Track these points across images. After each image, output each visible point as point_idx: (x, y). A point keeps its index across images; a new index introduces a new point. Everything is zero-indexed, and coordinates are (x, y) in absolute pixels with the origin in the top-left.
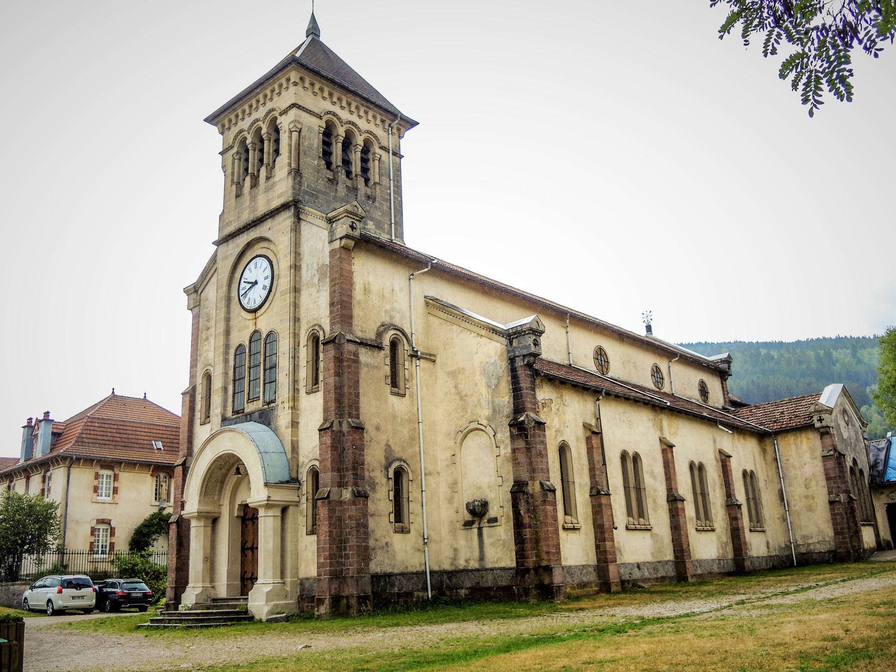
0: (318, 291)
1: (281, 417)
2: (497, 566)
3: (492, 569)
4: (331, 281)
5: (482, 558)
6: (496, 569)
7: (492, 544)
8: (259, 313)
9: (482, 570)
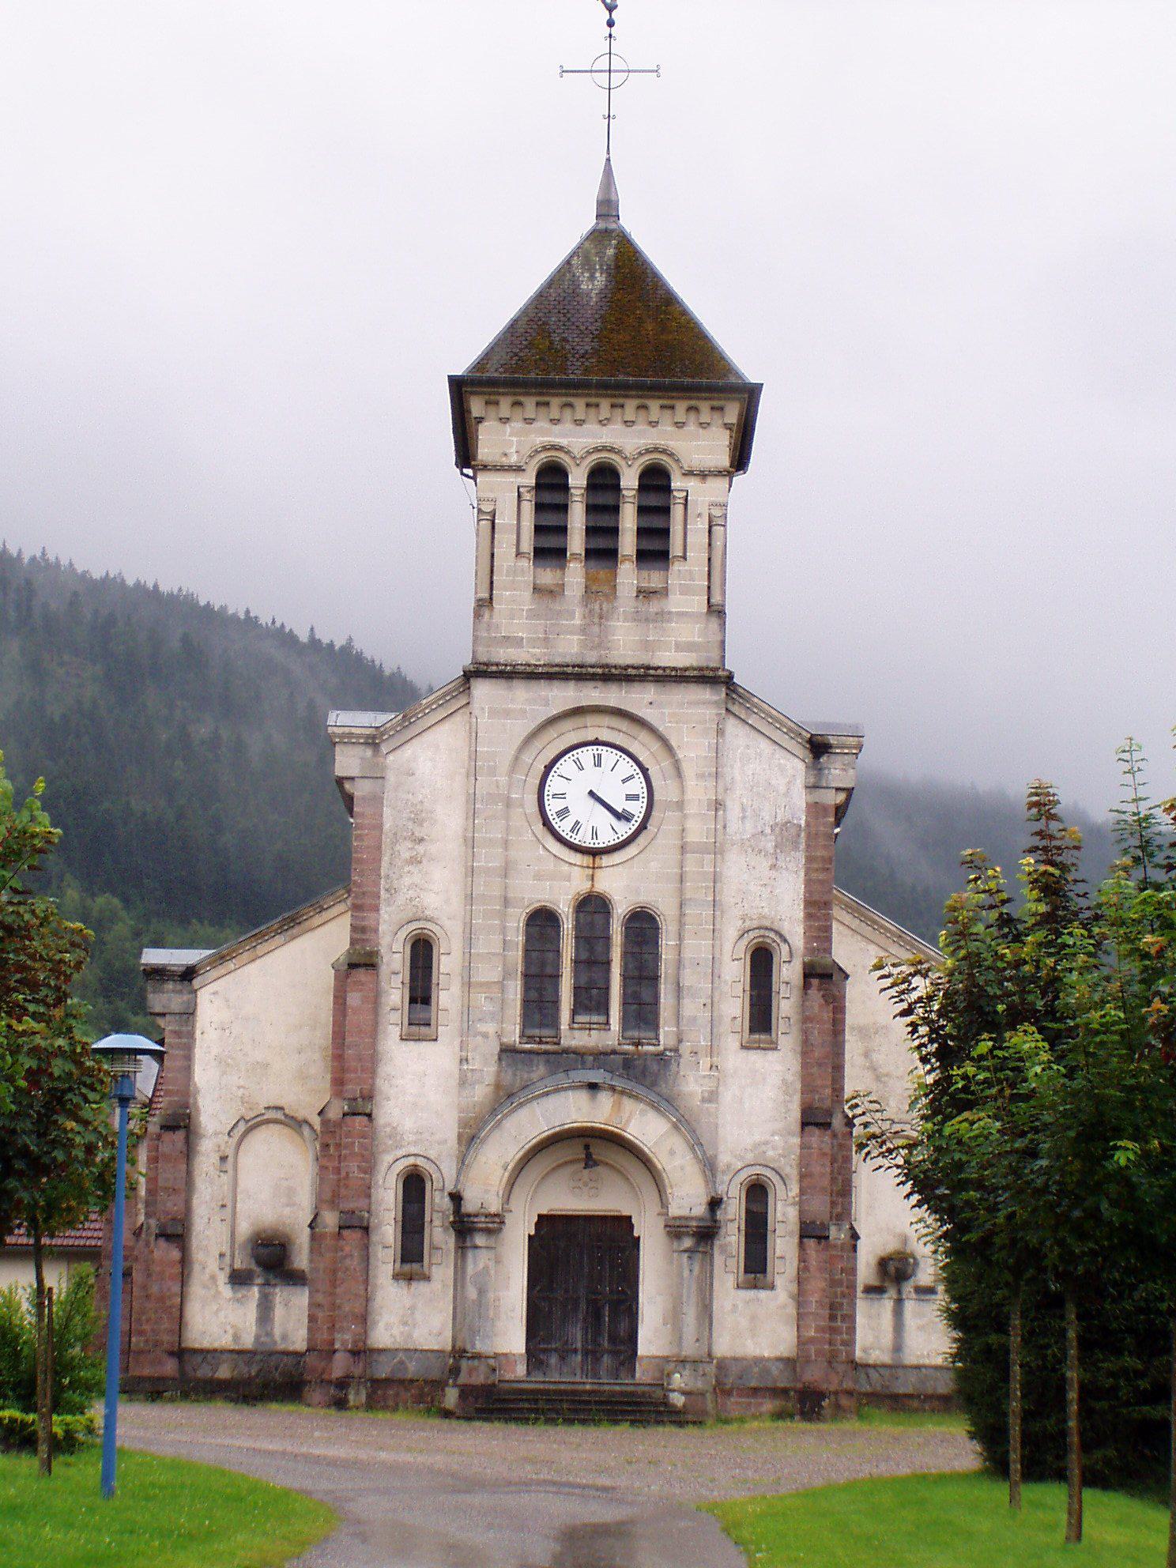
0: (773, 867)
1: (691, 1079)
2: (927, 1362)
3: (918, 1367)
4: (810, 859)
5: (898, 1347)
6: (925, 1367)
7: (921, 1328)
8: (606, 860)
9: (896, 1367)
